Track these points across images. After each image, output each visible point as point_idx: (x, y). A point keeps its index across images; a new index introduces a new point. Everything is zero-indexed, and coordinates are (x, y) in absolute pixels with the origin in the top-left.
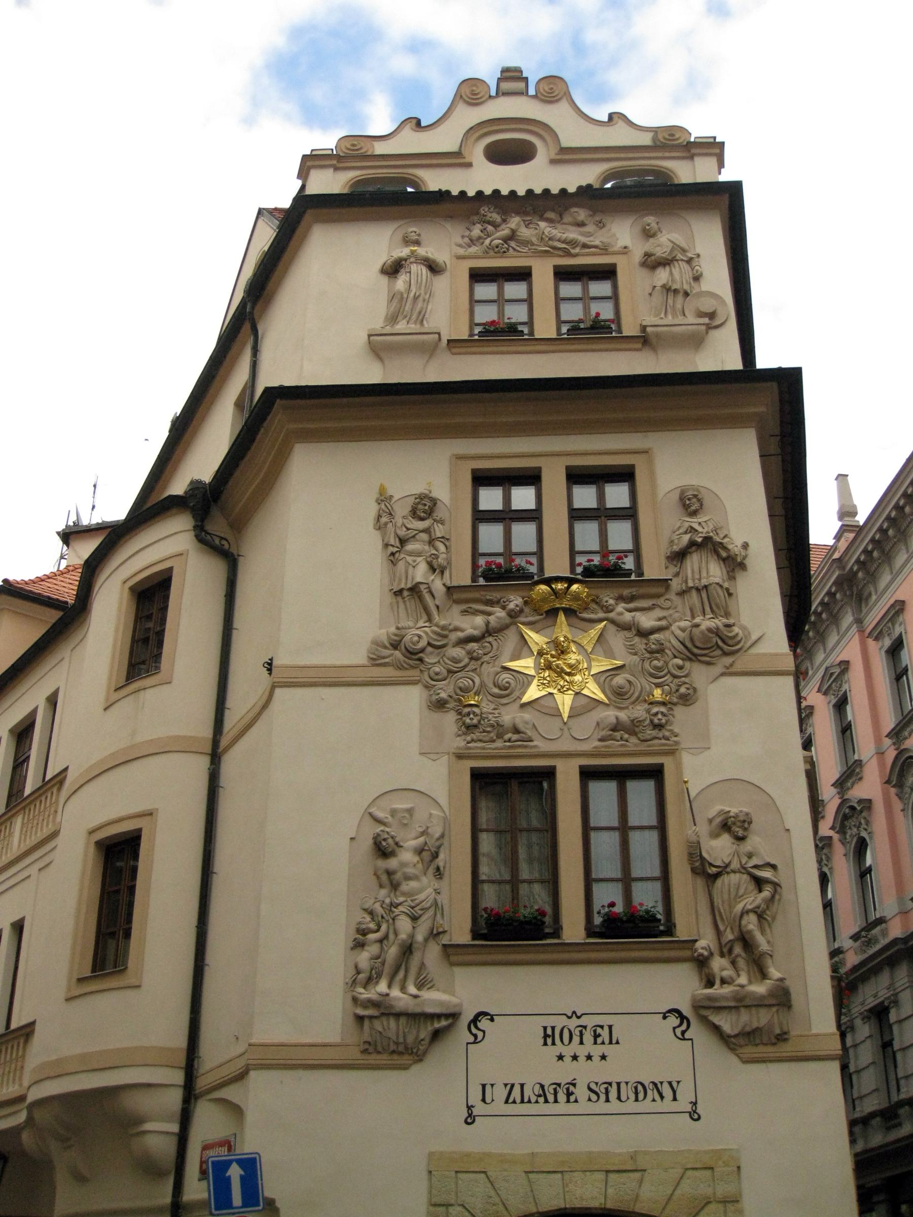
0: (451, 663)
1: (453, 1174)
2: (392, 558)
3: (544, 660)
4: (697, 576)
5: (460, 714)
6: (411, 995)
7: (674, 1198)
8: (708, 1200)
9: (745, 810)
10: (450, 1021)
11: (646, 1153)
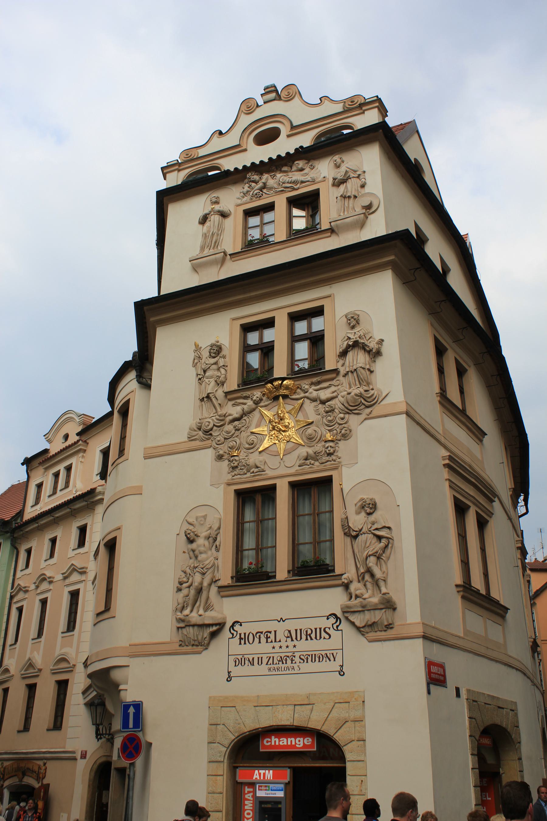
2: (200, 381)
3: (272, 425)
5: (229, 461)
6: (199, 615)
7: (329, 718)
8: (346, 720)
9: (371, 497)
10: (218, 627)
11: (315, 694)
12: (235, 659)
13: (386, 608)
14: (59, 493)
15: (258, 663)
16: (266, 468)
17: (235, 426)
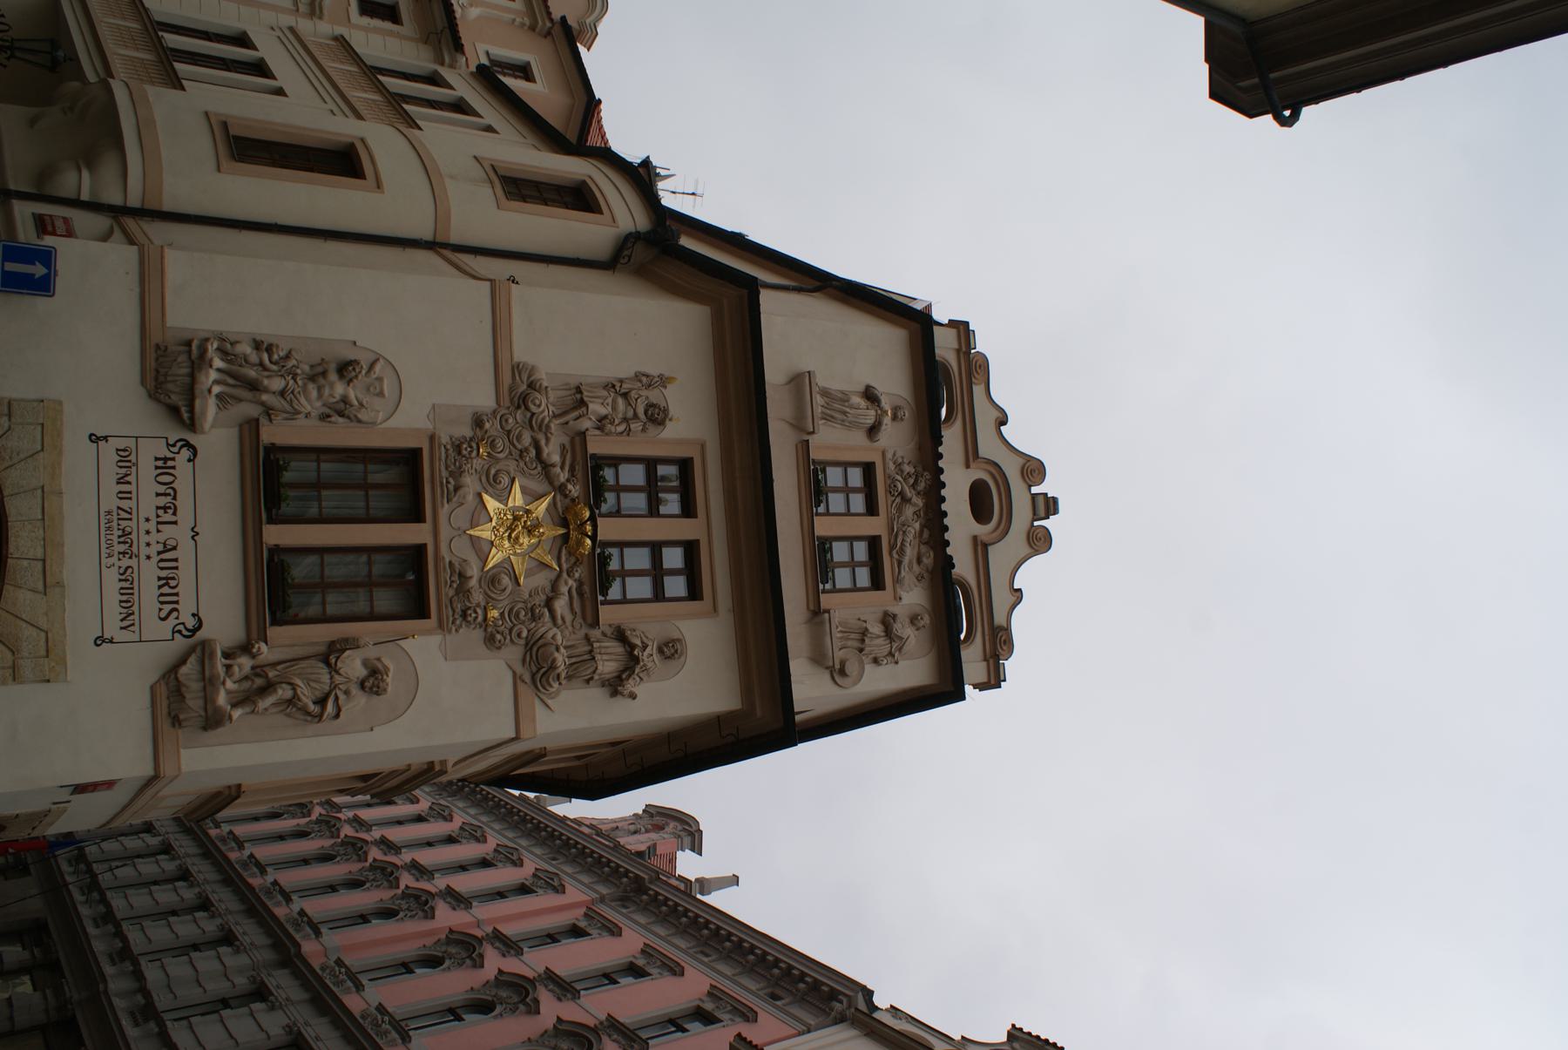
1: (41, 421)
2: (610, 386)
4: (603, 651)
5: (471, 439)
6: (211, 387)
9: (389, 689)
10: (188, 422)
13: (207, 718)
15: (120, 492)
16: (454, 503)
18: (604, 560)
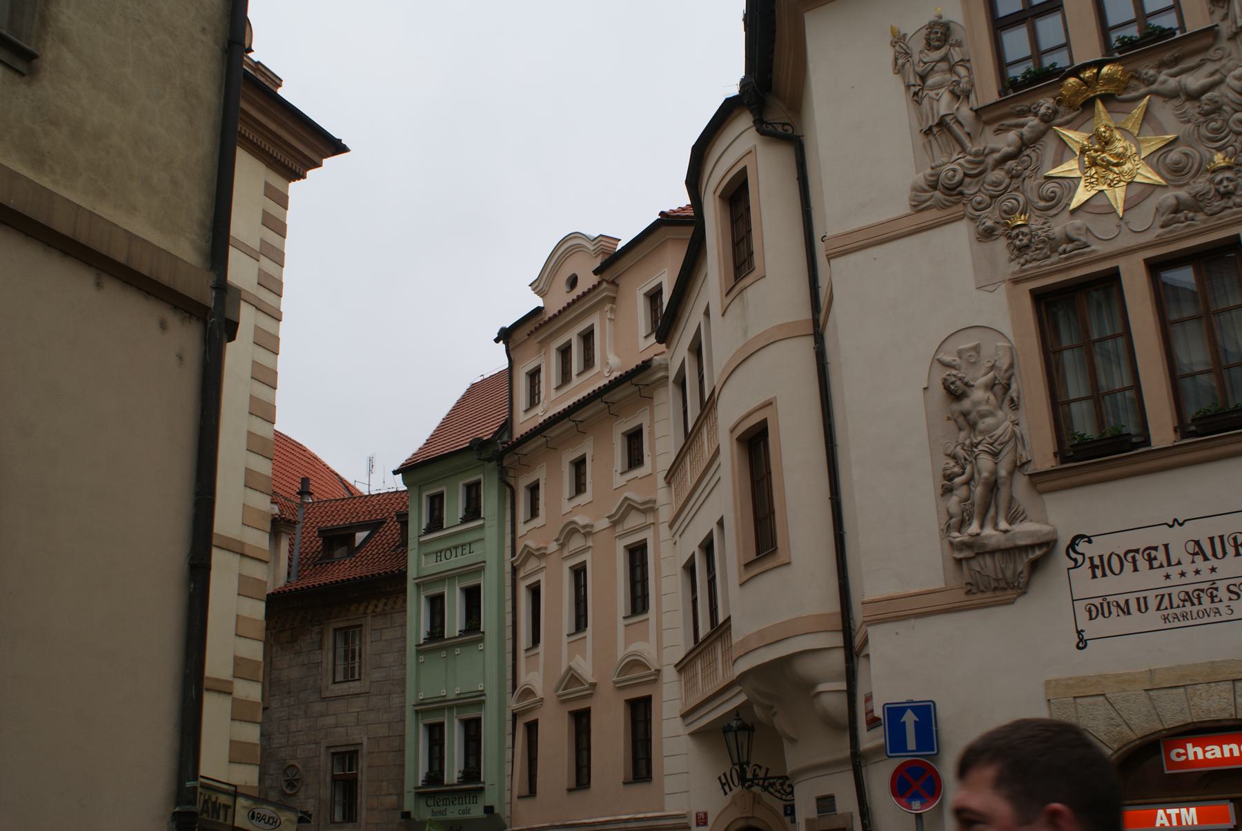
0: (991, 188)
2: (916, 98)
3: (1088, 157)
5: (1009, 237)
6: (1001, 531)
10: (1044, 550)
12: (1089, 606)
14: (575, 381)
16: (1090, 240)
17: (1009, 169)
18: (1127, 44)
